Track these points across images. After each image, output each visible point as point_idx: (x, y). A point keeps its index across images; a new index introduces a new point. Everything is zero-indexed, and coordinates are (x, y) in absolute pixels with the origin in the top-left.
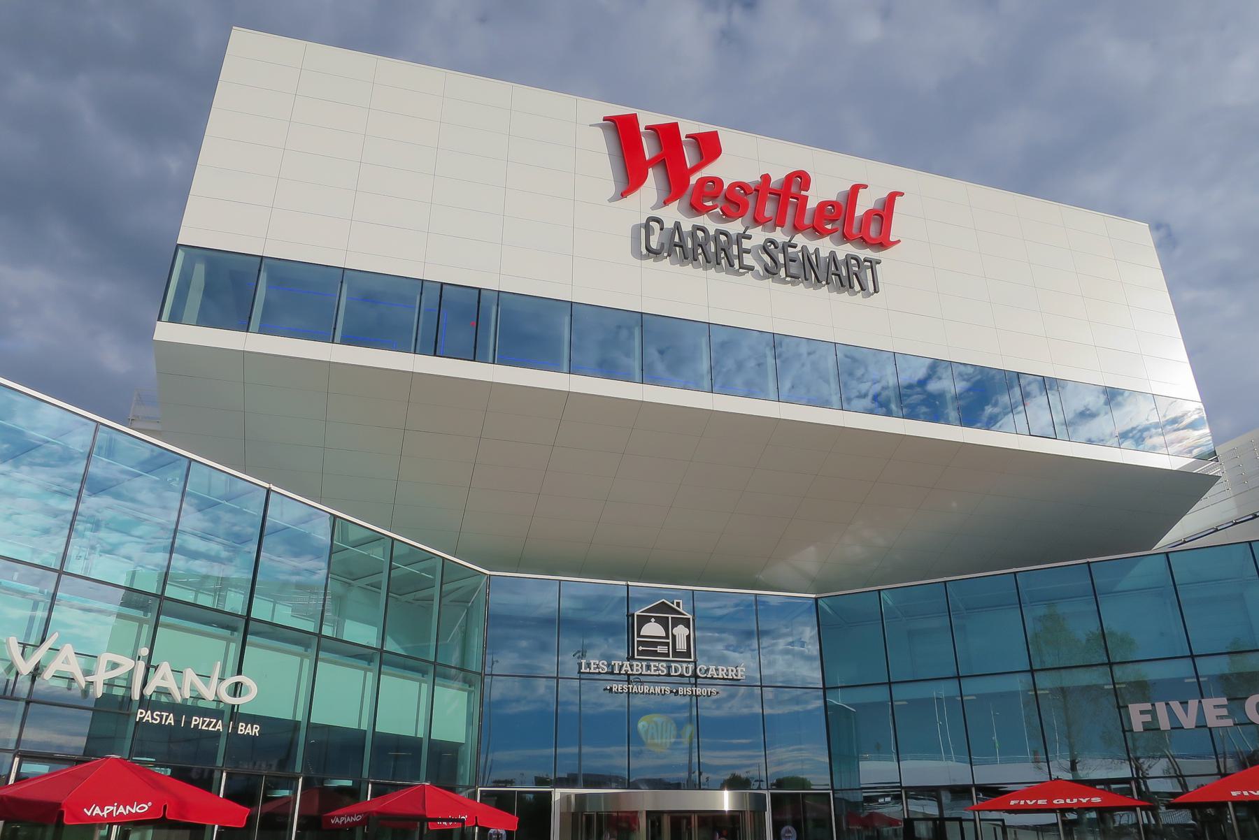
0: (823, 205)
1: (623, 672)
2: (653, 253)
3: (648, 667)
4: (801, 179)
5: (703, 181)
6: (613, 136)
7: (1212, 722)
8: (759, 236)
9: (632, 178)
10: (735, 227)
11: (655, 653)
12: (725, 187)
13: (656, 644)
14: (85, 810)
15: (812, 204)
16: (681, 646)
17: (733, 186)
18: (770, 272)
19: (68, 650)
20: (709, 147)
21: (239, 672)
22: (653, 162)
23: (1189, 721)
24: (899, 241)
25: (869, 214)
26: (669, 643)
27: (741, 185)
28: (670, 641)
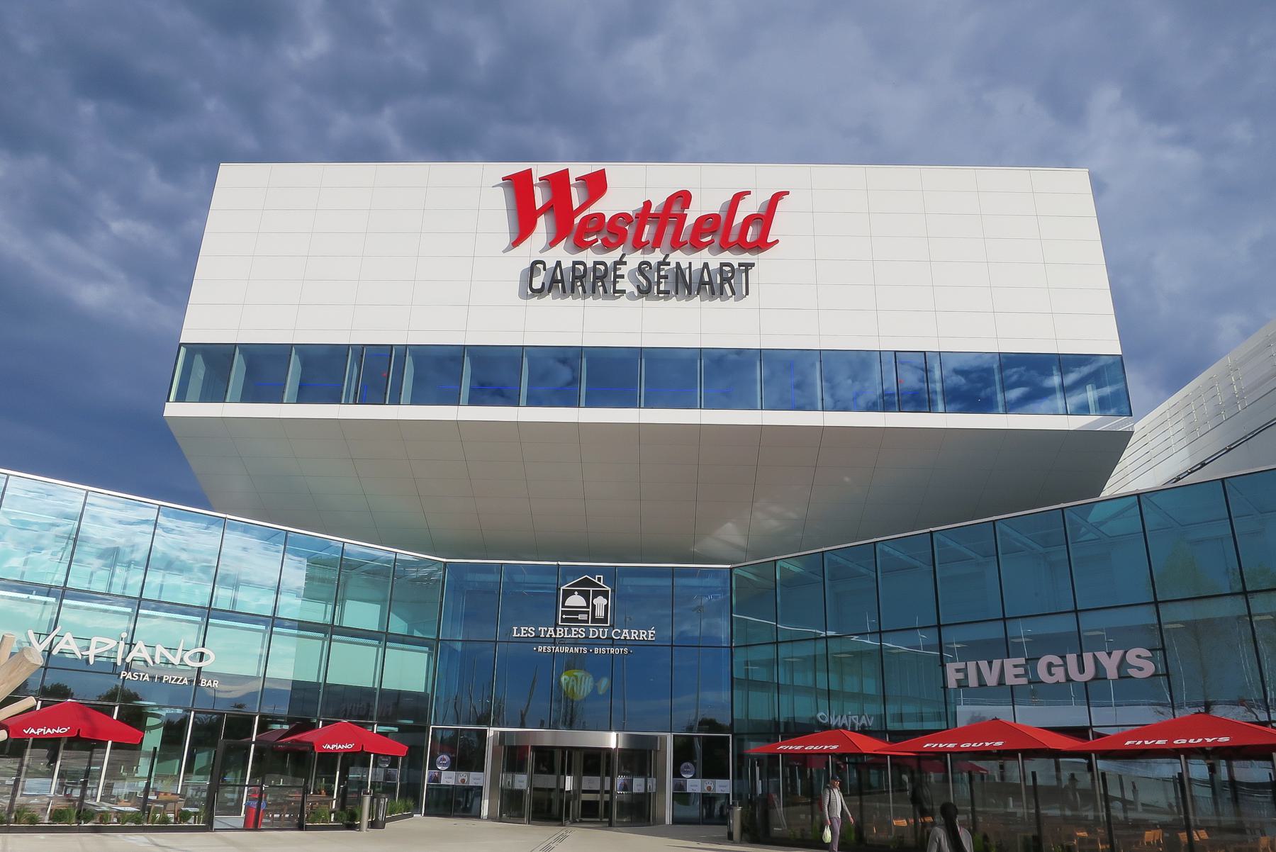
0: (701, 220)
1: (548, 636)
2: (539, 292)
3: (569, 632)
4: (683, 198)
6: (511, 192)
7: (1010, 680)
8: (634, 259)
9: (524, 228)
10: (611, 257)
11: (577, 620)
12: (607, 220)
13: (577, 613)
14: (24, 730)
15: (690, 220)
16: (600, 613)
18: (644, 292)
19: (68, 636)
20: (596, 185)
21: (203, 646)
22: (544, 210)
23: (991, 680)
24: (777, 241)
25: (749, 221)
26: (589, 611)
27: (625, 216)
28: (590, 610)
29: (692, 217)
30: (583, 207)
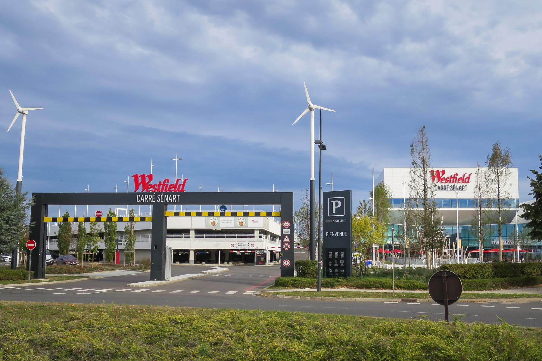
0: (459, 178)
4: (457, 174)
8: (450, 184)
10: (446, 184)
15: (458, 178)
20: (443, 172)
22: (436, 177)
25: (466, 178)
27: (448, 178)
29: (458, 177)
30: (442, 176)
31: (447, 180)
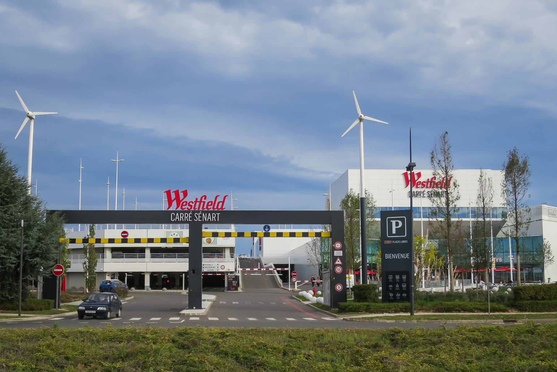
5: (418, 183)
8: (427, 190)
10: (422, 190)
12: (422, 182)
17: (423, 182)
27: (425, 182)
31: (423, 185)
